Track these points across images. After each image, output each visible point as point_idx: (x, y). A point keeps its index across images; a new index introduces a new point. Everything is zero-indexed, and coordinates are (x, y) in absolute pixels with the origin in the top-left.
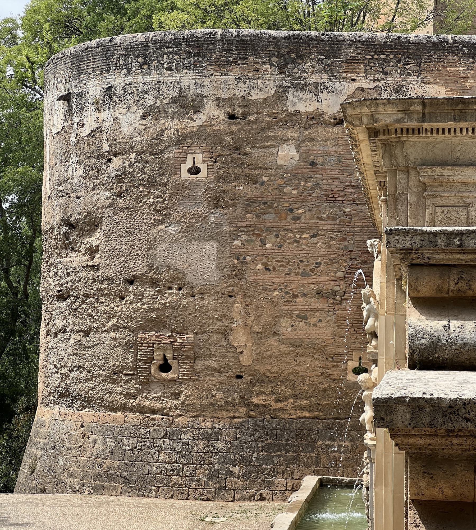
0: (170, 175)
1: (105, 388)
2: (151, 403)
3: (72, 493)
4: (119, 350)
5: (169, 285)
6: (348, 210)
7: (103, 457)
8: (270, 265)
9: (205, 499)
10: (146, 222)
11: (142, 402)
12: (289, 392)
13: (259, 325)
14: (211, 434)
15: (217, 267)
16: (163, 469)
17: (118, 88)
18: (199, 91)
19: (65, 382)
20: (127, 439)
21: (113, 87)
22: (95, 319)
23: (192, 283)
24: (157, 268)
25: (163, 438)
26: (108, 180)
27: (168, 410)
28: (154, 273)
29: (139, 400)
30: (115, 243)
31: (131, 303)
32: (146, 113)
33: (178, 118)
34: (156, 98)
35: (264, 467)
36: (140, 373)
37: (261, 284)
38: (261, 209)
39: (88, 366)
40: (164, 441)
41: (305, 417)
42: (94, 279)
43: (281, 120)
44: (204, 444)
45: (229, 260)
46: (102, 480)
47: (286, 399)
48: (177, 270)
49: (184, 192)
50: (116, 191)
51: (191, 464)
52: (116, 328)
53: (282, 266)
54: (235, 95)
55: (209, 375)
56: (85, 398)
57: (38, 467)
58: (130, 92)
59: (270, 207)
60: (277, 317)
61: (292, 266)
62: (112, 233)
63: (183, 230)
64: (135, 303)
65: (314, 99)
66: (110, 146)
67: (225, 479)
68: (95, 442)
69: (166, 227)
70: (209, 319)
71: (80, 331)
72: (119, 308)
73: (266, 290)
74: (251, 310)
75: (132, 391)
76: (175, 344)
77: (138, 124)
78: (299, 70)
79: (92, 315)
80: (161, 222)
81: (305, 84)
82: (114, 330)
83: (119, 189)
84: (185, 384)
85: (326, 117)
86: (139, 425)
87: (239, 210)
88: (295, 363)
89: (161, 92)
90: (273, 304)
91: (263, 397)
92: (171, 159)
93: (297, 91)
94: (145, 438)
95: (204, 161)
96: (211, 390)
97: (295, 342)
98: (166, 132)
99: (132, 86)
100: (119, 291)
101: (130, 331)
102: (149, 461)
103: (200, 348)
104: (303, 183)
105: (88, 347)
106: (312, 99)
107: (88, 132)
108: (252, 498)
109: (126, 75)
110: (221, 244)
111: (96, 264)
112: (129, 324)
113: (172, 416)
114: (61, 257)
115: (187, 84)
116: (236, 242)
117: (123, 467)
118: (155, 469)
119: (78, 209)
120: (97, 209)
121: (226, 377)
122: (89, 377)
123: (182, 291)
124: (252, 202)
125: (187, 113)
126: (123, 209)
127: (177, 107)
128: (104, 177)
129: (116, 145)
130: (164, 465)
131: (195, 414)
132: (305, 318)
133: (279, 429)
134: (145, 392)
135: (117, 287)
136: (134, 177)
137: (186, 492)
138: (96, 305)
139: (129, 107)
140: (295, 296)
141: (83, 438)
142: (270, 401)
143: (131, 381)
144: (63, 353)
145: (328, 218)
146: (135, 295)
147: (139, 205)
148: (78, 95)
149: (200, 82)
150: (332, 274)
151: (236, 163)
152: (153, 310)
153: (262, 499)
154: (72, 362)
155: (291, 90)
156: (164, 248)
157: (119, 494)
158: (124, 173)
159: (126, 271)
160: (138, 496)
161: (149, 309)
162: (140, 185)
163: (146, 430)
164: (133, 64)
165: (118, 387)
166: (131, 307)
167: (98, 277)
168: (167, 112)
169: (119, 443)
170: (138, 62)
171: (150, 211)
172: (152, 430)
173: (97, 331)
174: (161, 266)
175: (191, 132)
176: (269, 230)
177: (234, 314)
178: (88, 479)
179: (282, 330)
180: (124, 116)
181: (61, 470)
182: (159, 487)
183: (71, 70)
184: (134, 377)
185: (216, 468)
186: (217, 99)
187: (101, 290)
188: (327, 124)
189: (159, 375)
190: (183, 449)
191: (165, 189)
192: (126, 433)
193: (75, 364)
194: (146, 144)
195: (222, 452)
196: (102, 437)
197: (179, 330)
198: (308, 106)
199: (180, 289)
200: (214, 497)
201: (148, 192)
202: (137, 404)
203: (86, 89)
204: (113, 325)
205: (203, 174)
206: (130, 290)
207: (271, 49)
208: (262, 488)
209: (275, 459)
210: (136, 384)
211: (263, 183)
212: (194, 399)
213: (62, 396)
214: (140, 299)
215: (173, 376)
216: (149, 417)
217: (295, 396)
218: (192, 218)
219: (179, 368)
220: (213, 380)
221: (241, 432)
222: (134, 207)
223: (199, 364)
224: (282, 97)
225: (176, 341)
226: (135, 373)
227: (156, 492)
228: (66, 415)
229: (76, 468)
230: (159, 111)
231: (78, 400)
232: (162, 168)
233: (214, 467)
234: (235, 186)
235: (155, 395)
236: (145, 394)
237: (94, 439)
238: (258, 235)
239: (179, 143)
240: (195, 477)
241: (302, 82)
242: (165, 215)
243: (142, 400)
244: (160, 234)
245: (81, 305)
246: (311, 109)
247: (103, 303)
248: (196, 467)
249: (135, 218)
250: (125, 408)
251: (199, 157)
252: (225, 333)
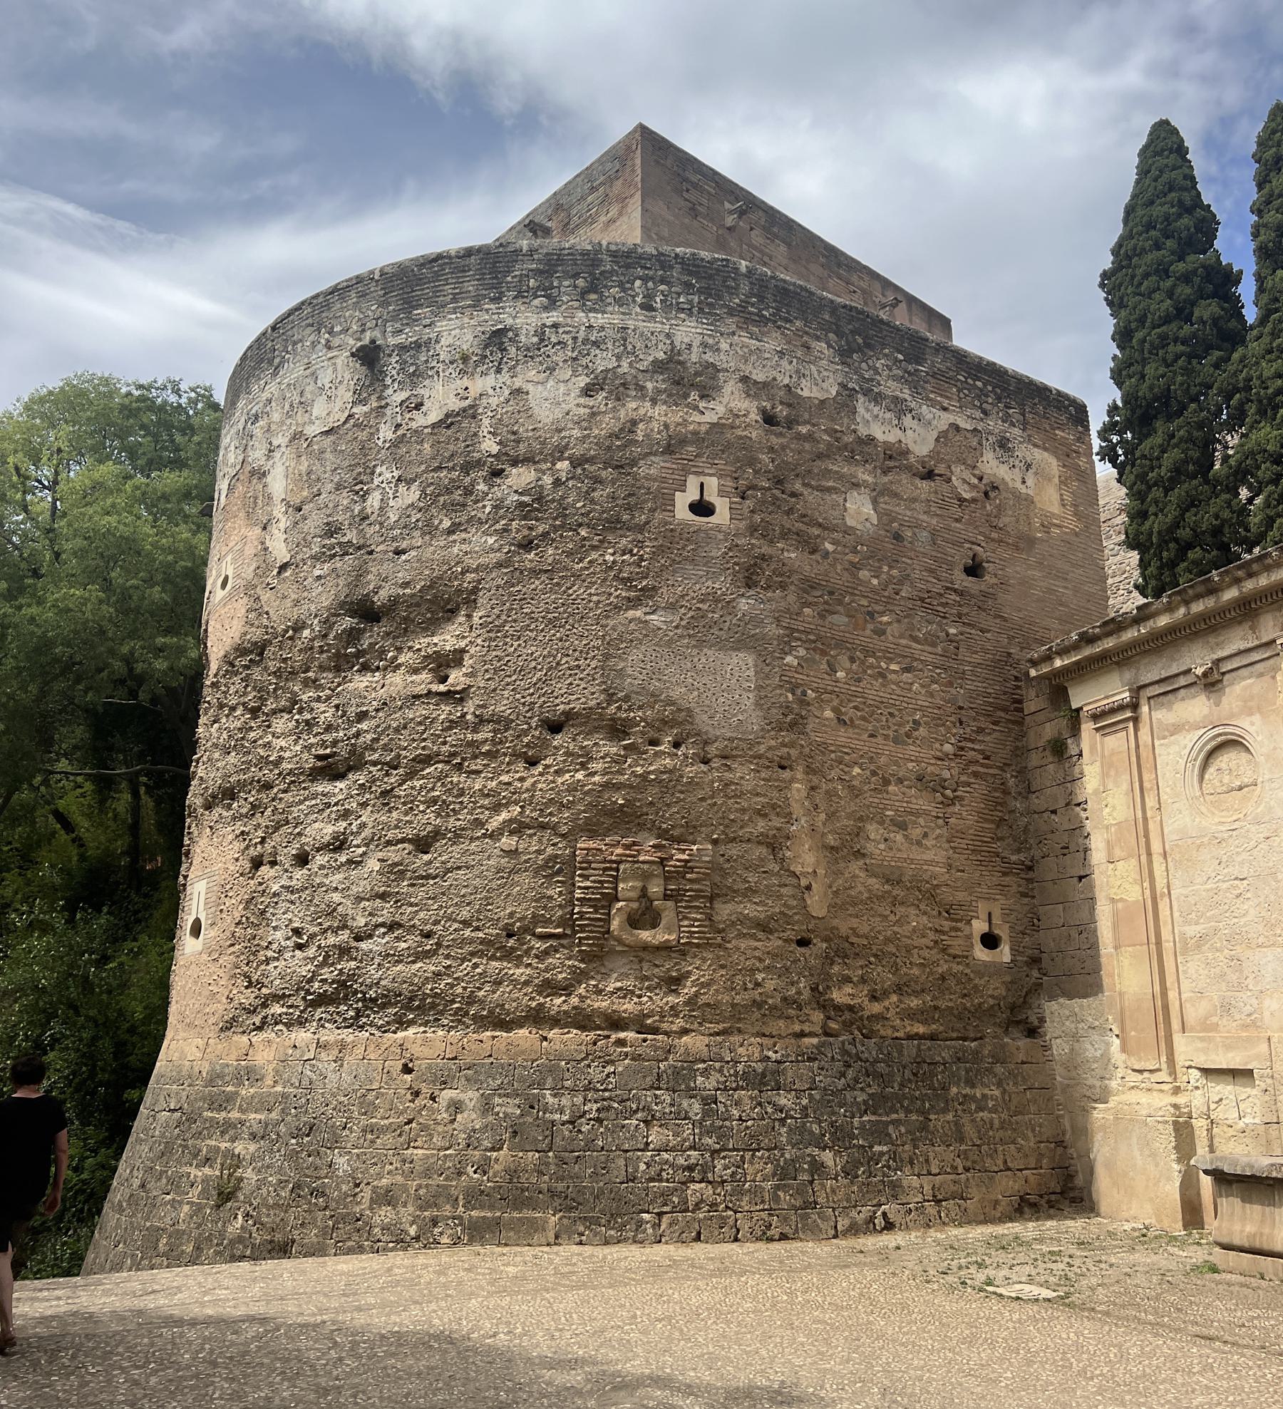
0: (653, 510)
1: (478, 970)
2: (613, 1003)
3: (392, 1250)
4: (525, 879)
5: (652, 734)
6: (952, 631)
7: (487, 1144)
8: (846, 714)
9: (777, 1237)
10: (599, 602)
11: (588, 1001)
12: (889, 979)
13: (833, 832)
14: (763, 1075)
15: (757, 704)
16: (666, 1167)
17: (524, 332)
18: (709, 357)
19: (339, 967)
20: (555, 1096)
21: (510, 330)
22: (453, 810)
23: (706, 733)
24: (627, 698)
25: (652, 1087)
26: (496, 513)
27: (657, 1018)
28: (619, 708)
29: (581, 997)
30: (516, 644)
31: (558, 773)
32: (594, 385)
33: (665, 402)
34: (619, 358)
35: (877, 1148)
36: (581, 932)
37: (832, 748)
38: (826, 603)
39: (425, 922)
40: (656, 1096)
41: (917, 1034)
42: (451, 721)
43: (845, 447)
44: (751, 1098)
45: (778, 691)
46: (492, 1207)
47: (886, 994)
48: (673, 704)
49: (683, 548)
50: (519, 536)
51: (729, 1150)
52: (517, 828)
53: (863, 718)
54: (775, 379)
55: (745, 935)
56: (411, 999)
57: (247, 1187)
58: (554, 340)
59: (840, 602)
60: (861, 819)
61: (878, 721)
62: (506, 621)
63: (683, 623)
64: (569, 771)
66: (500, 443)
67: (811, 1182)
68: (456, 1107)
69: (646, 614)
70: (743, 811)
71: (403, 841)
72: (527, 784)
73: (840, 763)
74: (819, 797)
75: (560, 976)
76: (672, 863)
77: (574, 404)
79: (444, 801)
80: (634, 603)
82: (512, 833)
83: (526, 532)
84: (696, 956)
86: (583, 1059)
87: (792, 598)
88: (892, 917)
89: (630, 347)
90: (855, 792)
91: (848, 989)
92: (655, 480)
94: (605, 1090)
95: (722, 493)
96: (753, 971)
97: (892, 873)
98: (641, 426)
99: (561, 330)
100: (527, 745)
101: (556, 834)
102: (626, 1147)
103: (725, 875)
104: (885, 569)
105: (428, 877)
107: (434, 417)
108: (869, 1227)
109: (545, 309)
110: (764, 659)
111: (458, 688)
112: (555, 819)
113: (666, 1033)
114: (319, 687)
115: (686, 340)
116: (789, 659)
117: (552, 1167)
118: (643, 1167)
119: (400, 575)
120: (463, 573)
121: (780, 942)
122: (428, 947)
123: (683, 748)
124: (812, 587)
125: (686, 396)
126: (535, 573)
127: (663, 380)
128: (484, 507)
129: (519, 442)
130: (665, 1155)
131: (721, 1026)
132: (902, 826)
133: (883, 1061)
134: (593, 978)
135: (519, 736)
136: (565, 509)
137: (731, 1221)
138: (455, 780)
139: (552, 370)
140: (886, 782)
141: (412, 1101)
142: (862, 999)
143: (556, 951)
144: (336, 897)
145: (926, 639)
146: (568, 754)
147: (576, 566)
148: (403, 348)
149: (711, 341)
150: (937, 745)
151: (779, 507)
152: (618, 787)
153: (889, 1226)
154: (370, 914)
156: (641, 656)
157: (552, 1240)
158: (539, 499)
159: (545, 702)
160: (607, 1243)
161: (606, 786)
162: (580, 525)
163: (606, 1071)
164: (563, 289)
165: (517, 967)
166: (560, 780)
167: (463, 716)
168: (643, 388)
169: (532, 1107)
170: (575, 287)
171: (605, 580)
172: (620, 1069)
173: (457, 836)
174: (637, 693)
175: (695, 433)
176: (841, 644)
177: (793, 804)
178: (448, 1207)
179: (870, 847)
180: (540, 387)
181: (344, 1188)
182: (660, 1215)
183: (384, 304)
184: (564, 942)
185: (787, 1156)
186: (745, 379)
187: (471, 744)
189: (632, 935)
190: (706, 1114)
191: (640, 537)
192: (550, 1080)
193: (381, 920)
194: (596, 444)
195: (792, 1118)
196: (477, 1094)
197: (676, 833)
199: (677, 745)
200: (796, 1231)
201: (600, 541)
202: (575, 1008)
203: (433, 335)
204: (511, 821)
205: (722, 515)
206: (555, 743)
208: (883, 1200)
209: (891, 1129)
210: (569, 959)
211: (826, 555)
212: (716, 990)
213: (321, 1000)
214: (582, 764)
215: (666, 937)
216: (608, 1037)
217: (899, 989)
218: (702, 601)
219: (680, 920)
220: (756, 948)
221: (822, 1069)
222: (566, 568)
223: (725, 911)
224: (847, 406)
225: (671, 858)
226: (568, 932)
227: (653, 1226)
228: (342, 1046)
229: (399, 1179)
230: (624, 385)
231: (384, 1006)
232: (633, 495)
233: (782, 1155)
234: (782, 550)
235: (619, 984)
236: (593, 983)
237: (451, 1099)
238: (824, 653)
239: (669, 450)
240: (746, 1181)
242: (641, 590)
243: (587, 998)
244: (632, 626)
245: (404, 782)
247: (478, 772)
248: (742, 1156)
249: (570, 591)
250: (537, 1018)
251: (712, 483)
252: (774, 844)
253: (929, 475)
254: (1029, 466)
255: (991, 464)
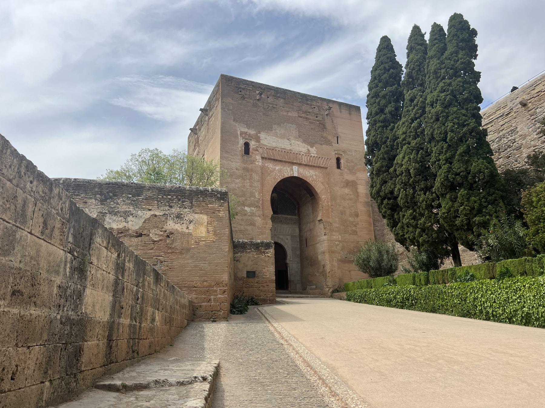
65: (123, 220)
78: (115, 203)
81: (118, 212)
85: (130, 232)
93: (112, 215)
106: (122, 221)
155: (108, 215)
188: (131, 236)
198: (119, 224)
207: (97, 190)
241: (116, 210)
246: (120, 226)
253: (141, 235)
254: (191, 222)
255: (171, 225)
